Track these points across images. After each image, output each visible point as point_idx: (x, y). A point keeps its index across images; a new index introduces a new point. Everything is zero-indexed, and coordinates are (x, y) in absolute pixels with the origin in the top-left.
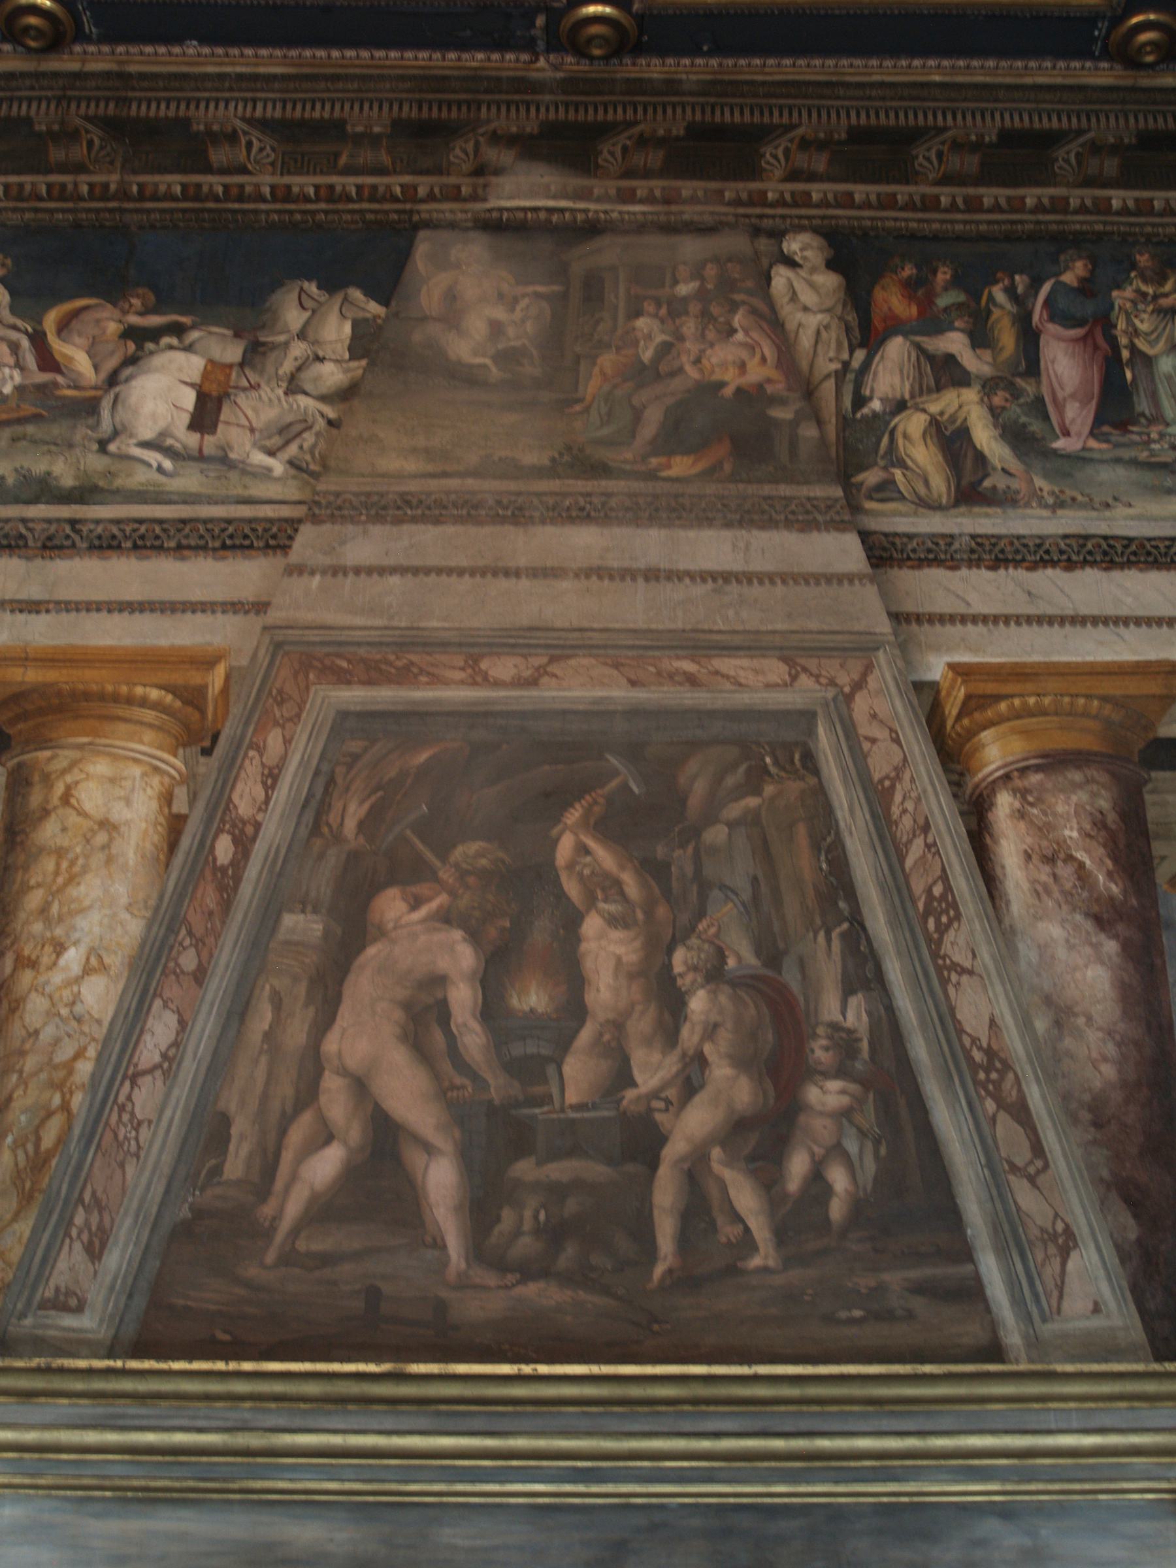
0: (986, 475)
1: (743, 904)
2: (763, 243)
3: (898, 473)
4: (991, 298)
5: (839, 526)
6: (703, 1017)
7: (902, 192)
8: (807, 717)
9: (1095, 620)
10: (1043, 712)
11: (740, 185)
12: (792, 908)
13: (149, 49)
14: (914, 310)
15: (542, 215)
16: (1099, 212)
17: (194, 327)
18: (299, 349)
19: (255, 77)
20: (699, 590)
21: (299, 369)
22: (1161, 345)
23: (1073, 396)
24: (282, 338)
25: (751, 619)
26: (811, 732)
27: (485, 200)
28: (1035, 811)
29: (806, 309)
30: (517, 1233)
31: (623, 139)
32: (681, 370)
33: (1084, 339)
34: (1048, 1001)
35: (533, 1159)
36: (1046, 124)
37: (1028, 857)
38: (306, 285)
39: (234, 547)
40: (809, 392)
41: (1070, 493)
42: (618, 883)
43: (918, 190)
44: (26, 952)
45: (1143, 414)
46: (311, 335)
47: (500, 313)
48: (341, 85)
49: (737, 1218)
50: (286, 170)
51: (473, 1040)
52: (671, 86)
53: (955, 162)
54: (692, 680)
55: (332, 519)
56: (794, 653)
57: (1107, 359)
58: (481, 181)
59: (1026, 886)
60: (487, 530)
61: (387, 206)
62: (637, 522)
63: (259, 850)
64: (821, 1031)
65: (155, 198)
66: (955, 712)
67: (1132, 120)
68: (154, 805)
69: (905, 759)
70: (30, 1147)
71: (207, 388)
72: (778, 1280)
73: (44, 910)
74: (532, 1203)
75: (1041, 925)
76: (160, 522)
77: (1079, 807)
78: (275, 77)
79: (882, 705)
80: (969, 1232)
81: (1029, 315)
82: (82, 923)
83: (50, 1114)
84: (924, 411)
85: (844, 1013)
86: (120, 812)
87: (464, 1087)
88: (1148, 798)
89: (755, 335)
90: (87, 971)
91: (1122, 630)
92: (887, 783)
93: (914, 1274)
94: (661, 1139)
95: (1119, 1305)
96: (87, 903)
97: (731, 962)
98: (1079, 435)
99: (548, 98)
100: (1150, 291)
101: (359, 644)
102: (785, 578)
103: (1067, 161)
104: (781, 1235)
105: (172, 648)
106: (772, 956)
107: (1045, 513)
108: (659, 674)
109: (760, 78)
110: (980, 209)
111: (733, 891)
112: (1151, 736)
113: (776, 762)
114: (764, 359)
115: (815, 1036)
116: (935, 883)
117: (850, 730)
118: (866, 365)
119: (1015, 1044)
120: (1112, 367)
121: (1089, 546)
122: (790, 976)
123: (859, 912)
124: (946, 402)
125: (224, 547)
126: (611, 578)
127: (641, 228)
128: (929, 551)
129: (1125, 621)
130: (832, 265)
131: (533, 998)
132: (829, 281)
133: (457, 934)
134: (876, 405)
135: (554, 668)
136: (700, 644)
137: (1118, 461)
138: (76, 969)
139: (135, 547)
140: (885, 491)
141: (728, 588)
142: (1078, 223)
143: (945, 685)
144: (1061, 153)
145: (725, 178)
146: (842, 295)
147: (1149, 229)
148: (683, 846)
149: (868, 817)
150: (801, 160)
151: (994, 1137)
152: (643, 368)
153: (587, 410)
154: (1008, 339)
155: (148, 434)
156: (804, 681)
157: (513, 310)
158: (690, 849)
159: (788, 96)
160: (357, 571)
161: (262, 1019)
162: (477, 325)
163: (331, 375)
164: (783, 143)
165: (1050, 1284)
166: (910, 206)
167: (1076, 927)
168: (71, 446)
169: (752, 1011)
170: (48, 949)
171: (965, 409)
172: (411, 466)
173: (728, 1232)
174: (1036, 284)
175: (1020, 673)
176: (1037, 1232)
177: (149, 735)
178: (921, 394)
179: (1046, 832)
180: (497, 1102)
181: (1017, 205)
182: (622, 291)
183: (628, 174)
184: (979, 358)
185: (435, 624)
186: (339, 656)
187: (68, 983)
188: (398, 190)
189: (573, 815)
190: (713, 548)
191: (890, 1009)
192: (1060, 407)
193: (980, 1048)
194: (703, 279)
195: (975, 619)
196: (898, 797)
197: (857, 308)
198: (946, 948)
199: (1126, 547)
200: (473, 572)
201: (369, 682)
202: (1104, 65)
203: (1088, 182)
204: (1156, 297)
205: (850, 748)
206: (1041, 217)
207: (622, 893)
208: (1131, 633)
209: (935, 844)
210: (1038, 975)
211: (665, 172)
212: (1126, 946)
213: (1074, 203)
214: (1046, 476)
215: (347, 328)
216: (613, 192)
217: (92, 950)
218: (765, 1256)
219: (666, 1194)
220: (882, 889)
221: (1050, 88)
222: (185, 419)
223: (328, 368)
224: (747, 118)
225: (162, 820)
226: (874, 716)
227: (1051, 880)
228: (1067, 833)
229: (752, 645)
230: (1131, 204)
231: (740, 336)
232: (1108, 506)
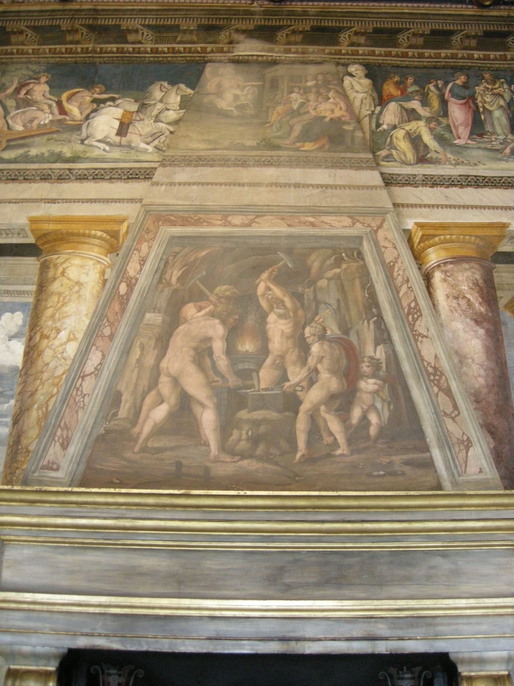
0: (428, 153)
1: (334, 309)
2: (340, 68)
3: (394, 152)
4: (429, 89)
5: (372, 168)
6: (317, 354)
7: (394, 51)
8: (360, 238)
9: (472, 207)
10: (452, 242)
11: (332, 48)
12: (354, 312)
15: (255, 58)
16: (469, 59)
17: (119, 99)
18: (160, 106)
19: (146, 10)
20: (316, 191)
21: (159, 113)
22: (495, 107)
23: (461, 124)
24: (153, 102)
25: (336, 202)
26: (361, 244)
28: (450, 279)
29: (357, 92)
30: (240, 440)
31: (286, 31)
32: (308, 112)
33: (465, 103)
35: (247, 410)
36: (448, 28)
37: (448, 297)
38: (163, 83)
39: (132, 178)
40: (359, 121)
41: (461, 159)
42: (282, 302)
44: (45, 333)
45: (488, 131)
46: (164, 100)
47: (238, 92)
48: (178, 13)
49: (331, 434)
50: (156, 42)
52: (305, 13)
53: (413, 41)
54: (313, 225)
55: (170, 165)
56: (354, 215)
57: (474, 112)
58: (232, 45)
59: (447, 308)
60: (231, 169)
61: (195, 55)
62: (291, 166)
63: (137, 289)
64: (366, 359)
65: (106, 52)
66: (418, 241)
67: (481, 26)
68: (98, 276)
69: (399, 255)
70: (44, 409)
71: (123, 120)
72: (348, 459)
73: (53, 316)
74: (246, 427)
75: (453, 323)
76: (104, 169)
79: (389, 234)
80: (428, 440)
82: (67, 321)
83: (52, 396)
84: (403, 129)
85: (375, 352)
86: (83, 279)
87: (218, 381)
88: (495, 275)
89: (338, 100)
90: (69, 340)
91: (483, 210)
92: (392, 264)
93: (405, 457)
94: (300, 403)
95: (490, 470)
96: (69, 314)
97: (329, 333)
98: (464, 138)
99: (257, 17)
100: (490, 87)
101: (180, 211)
102: (350, 187)
103: (456, 41)
104: (350, 441)
105: (107, 216)
108: (300, 222)
110: (424, 57)
111: (329, 305)
112: (495, 251)
113: (347, 255)
114: (341, 109)
115: (363, 362)
116: (412, 302)
117: (376, 244)
118: (381, 112)
119: (445, 365)
120: (476, 114)
121: (469, 179)
122: (353, 338)
123: (381, 313)
124: (412, 126)
125: (128, 178)
126: (281, 186)
128: (407, 180)
129: (484, 207)
130: (367, 76)
131: (247, 346)
132: (367, 82)
133: (217, 321)
134: (385, 127)
135: (256, 220)
136: (316, 211)
137: (480, 148)
138: (65, 340)
139: (94, 179)
140: (389, 158)
141: (327, 191)
142: (461, 63)
143: (413, 231)
144: (454, 38)
145: (326, 45)
146: (371, 86)
147: (488, 65)
148: (309, 287)
149: (384, 276)
150: (355, 39)
151: (437, 401)
152: (293, 111)
153: (271, 126)
154: (436, 103)
155: (100, 137)
156: (358, 225)
157: (243, 91)
158: (312, 289)
159: (349, 17)
160: (180, 184)
161: (136, 353)
162: (229, 96)
163: (172, 115)
164: (348, 33)
165: (462, 461)
166: (397, 56)
167: (467, 324)
168: (70, 142)
169: (337, 352)
170: (54, 331)
171: (420, 128)
172: (202, 146)
173: (328, 440)
174: (446, 83)
175: (443, 227)
176: (456, 440)
177: (96, 249)
178: (402, 123)
179: (454, 290)
180: (232, 387)
181: (438, 56)
182: (286, 84)
184: (425, 110)
185: (210, 203)
186: (171, 215)
187: (61, 345)
188: (199, 49)
189: (265, 275)
190: (321, 176)
191: (394, 351)
192: (456, 128)
193: (431, 367)
194: (317, 80)
195: (425, 206)
196: (396, 269)
197: (377, 92)
198: (417, 327)
199: (484, 180)
200: (225, 184)
201: (183, 225)
202: (470, 6)
203: (465, 48)
204: (492, 89)
205: (377, 250)
206: (447, 60)
207: (284, 305)
208: (486, 212)
209: (411, 287)
210: (452, 343)
211: (303, 43)
212: (487, 331)
213: (460, 56)
214: (452, 153)
215: (179, 98)
216: (282, 50)
217: (71, 332)
218: (343, 449)
219: (302, 425)
220: (391, 305)
221: (450, 15)
222: (115, 131)
223: (171, 112)
224: (334, 24)
225: (101, 281)
226: (386, 238)
227: (457, 306)
228: (463, 287)
229: (337, 212)
230: (481, 56)
231: (331, 100)
232: (476, 164)
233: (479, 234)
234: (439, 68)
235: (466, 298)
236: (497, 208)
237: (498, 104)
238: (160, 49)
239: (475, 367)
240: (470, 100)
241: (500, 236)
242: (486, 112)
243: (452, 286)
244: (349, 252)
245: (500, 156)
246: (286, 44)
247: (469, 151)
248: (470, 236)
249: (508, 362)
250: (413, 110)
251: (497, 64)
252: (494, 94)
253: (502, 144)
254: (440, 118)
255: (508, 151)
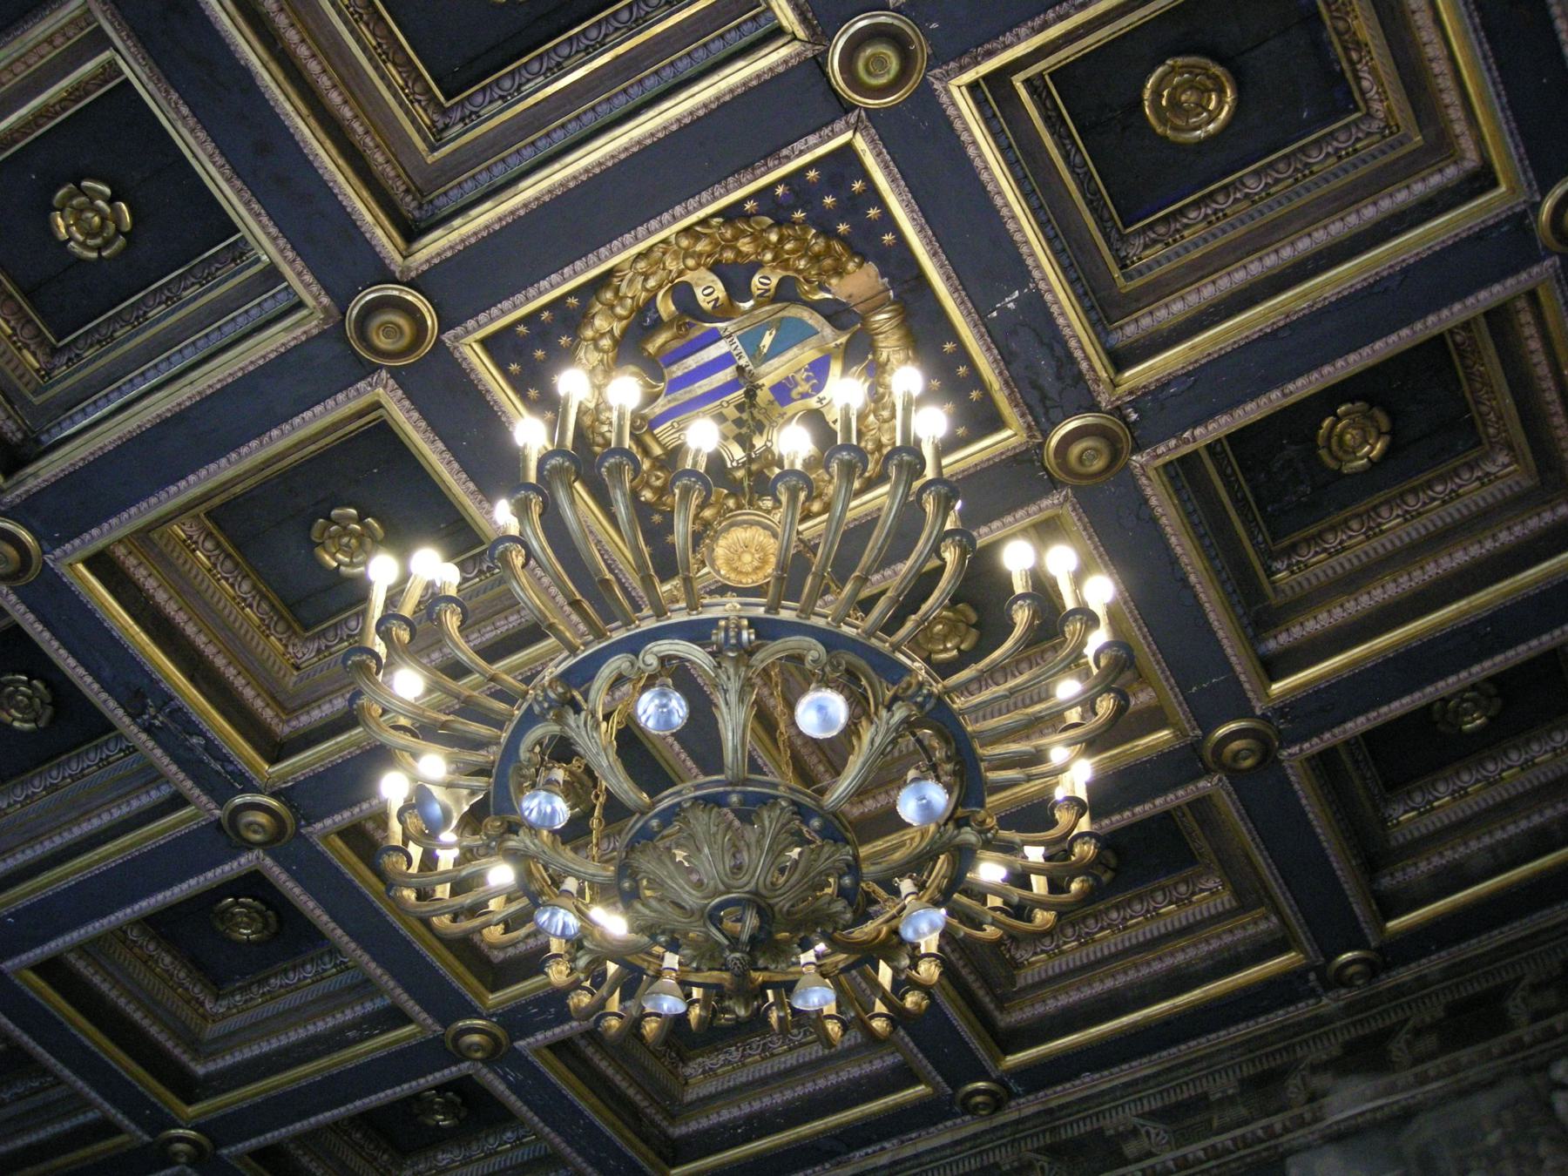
2: (1537, 1080)
11: (1500, 1039)
13: (1059, 1088)
19: (1135, 1082)
27: (1322, 1119)
31: (1403, 1036)
48: (1195, 1067)
52: (1422, 981)
58: (1315, 1105)
61: (1258, 1148)
78: (1146, 1079)
99: (1338, 1024)
109: (1480, 951)
183: (1418, 1061)
188: (1260, 1133)
216: (1411, 1079)
246: (1414, 1065)
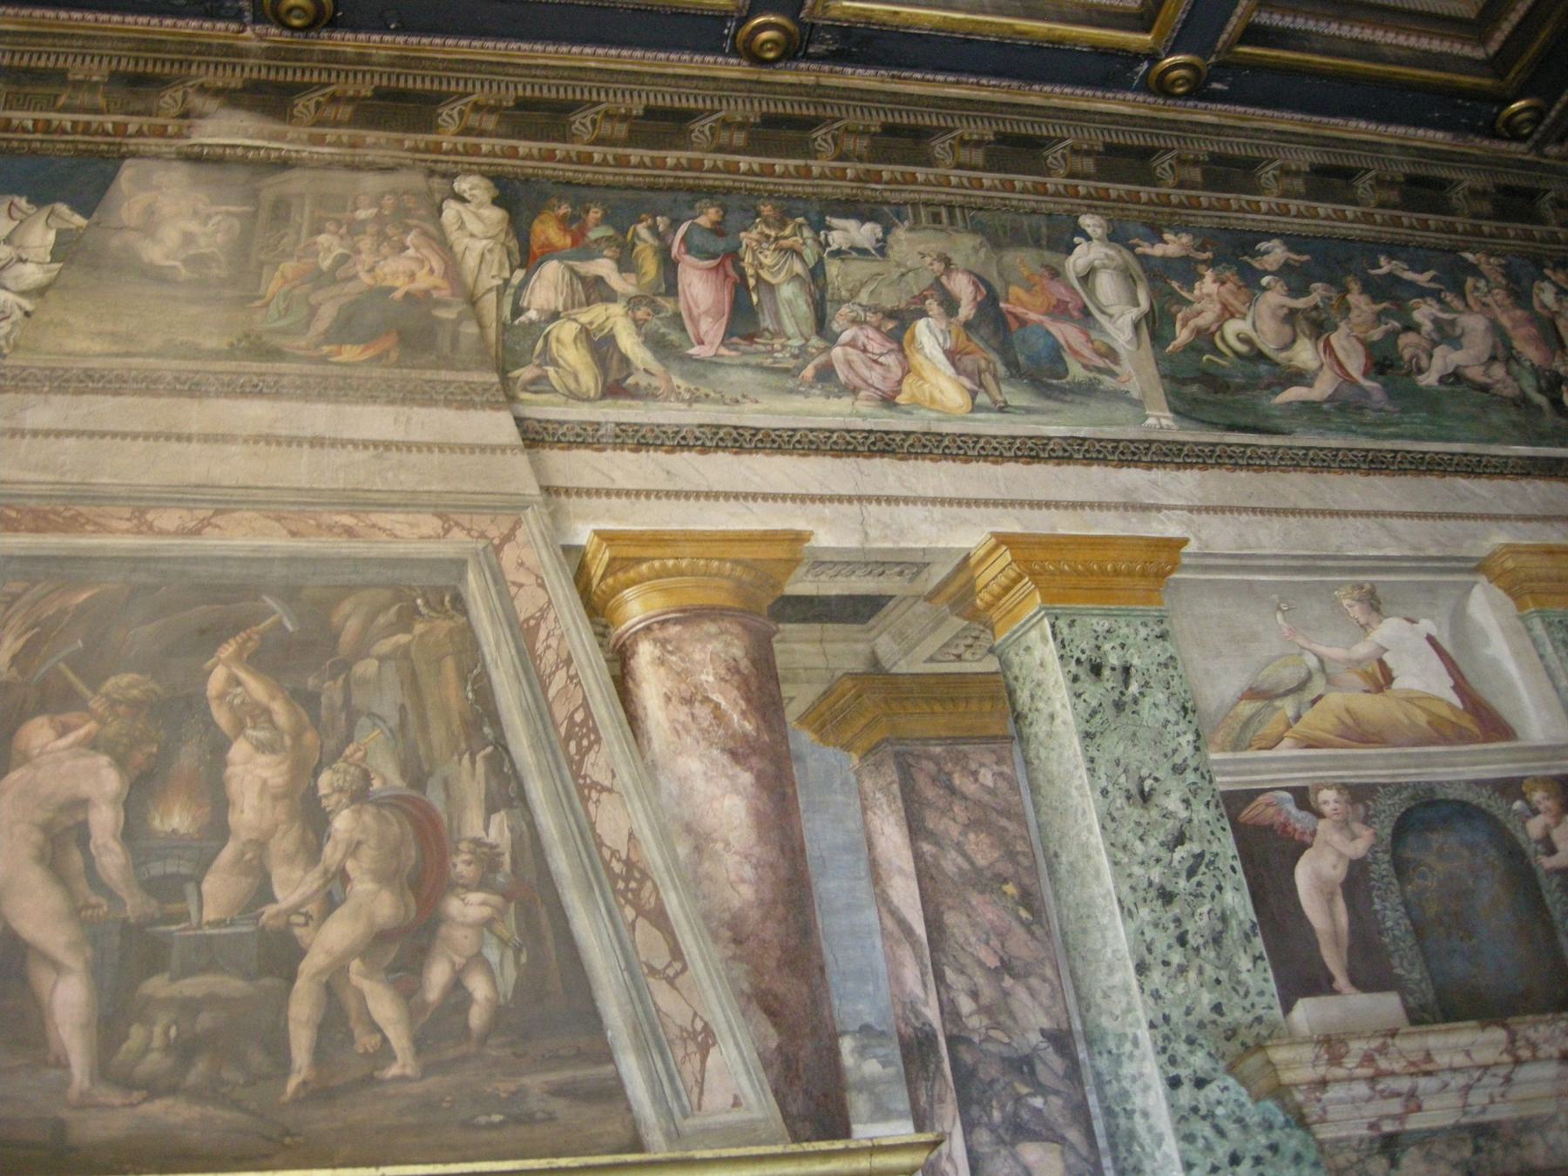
1: (391, 730)
2: (437, 182)
3: (551, 370)
4: (636, 235)
5: (495, 406)
6: (346, 835)
7: (560, 149)
8: (460, 565)
9: (727, 496)
10: (681, 574)
11: (419, 136)
12: (438, 734)
14: (569, 240)
15: (240, 151)
16: (729, 172)
20: (361, 456)
23: (706, 313)
25: (408, 481)
26: (462, 577)
27: (188, 137)
28: (674, 658)
29: (472, 235)
31: (316, 97)
32: (355, 277)
33: (716, 268)
34: (688, 829)
35: (167, 975)
36: (684, 104)
37: (668, 699)
38: (16, 199)
40: (473, 301)
41: (704, 390)
42: (267, 712)
43: (575, 148)
46: (17, 241)
47: (193, 226)
48: (66, 42)
49: (375, 1028)
51: (112, 859)
52: (362, 59)
53: (606, 128)
54: (350, 532)
55: (16, 389)
56: (448, 511)
57: (735, 284)
58: (187, 122)
59: (666, 725)
60: (163, 401)
61: (99, 139)
62: (306, 398)
64: (464, 846)
66: (600, 572)
69: (550, 602)
72: (416, 1088)
75: (680, 760)
77: (714, 656)
79: (529, 553)
80: (609, 1033)
81: (668, 249)
84: (575, 320)
85: (486, 828)
87: (98, 906)
88: (777, 647)
89: (426, 252)
91: (751, 503)
92: (532, 622)
93: (554, 1077)
94: (301, 953)
95: (759, 1101)
97: (376, 784)
98: (712, 344)
99: (252, 61)
100: (773, 234)
101: (30, 497)
102: (441, 447)
104: (419, 1044)
106: (417, 777)
107: (683, 406)
108: (319, 526)
109: (440, 56)
110: (628, 165)
111: (380, 718)
112: (778, 594)
113: (427, 603)
114: (432, 271)
115: (457, 851)
116: (577, 710)
117: (498, 577)
118: (524, 283)
119: (652, 854)
121: (721, 434)
122: (435, 797)
123: (503, 736)
124: (595, 314)
126: (279, 443)
127: (328, 165)
128: (578, 435)
130: (496, 202)
131: (176, 819)
132: (496, 215)
133: (104, 760)
134: (532, 314)
135: (217, 520)
136: (359, 501)
137: (746, 365)
140: (539, 384)
141: (388, 454)
142: (710, 179)
143: (591, 550)
144: (696, 126)
145: (406, 131)
146: (505, 225)
148: (334, 678)
149: (513, 651)
150: (473, 120)
151: (633, 942)
152: (321, 273)
153: (267, 305)
154: (650, 266)
156: (457, 534)
157: (206, 224)
158: (340, 681)
159: (464, 71)
160: (35, 433)
162: (171, 235)
163: (32, 274)
164: (458, 106)
165: (690, 1080)
166: (567, 159)
167: (713, 761)
169: (396, 829)
171: (612, 320)
173: (366, 1042)
174: (675, 223)
175: (659, 539)
176: (676, 1031)
178: (573, 307)
179: (684, 678)
182: (307, 210)
183: (320, 123)
185: (105, 480)
186: (8, 506)
188: (110, 127)
189: (228, 650)
190: (377, 421)
191: (532, 825)
192: (695, 322)
193: (619, 860)
194: (381, 207)
195: (618, 493)
196: (542, 634)
197: (518, 236)
198: (587, 768)
200: (147, 437)
201: (37, 530)
202: (733, 61)
203: (720, 149)
204: (777, 239)
205: (499, 593)
206: (680, 173)
207: (271, 721)
208: (759, 507)
209: (577, 675)
210: (679, 805)
211: (353, 122)
212: (759, 777)
213: (708, 164)
214: (683, 375)
215: (52, 236)
216: (305, 137)
218: (403, 1063)
219: (302, 1008)
220: (527, 720)
221: (687, 77)
224: (428, 86)
226: (521, 564)
228: (703, 677)
229: (410, 503)
230: (756, 167)
231: (411, 252)
233: (742, 556)
234: (660, 189)
235: (711, 700)
236: (784, 497)
237: (790, 270)
238: (15, 123)
239: (731, 860)
240: (727, 262)
241: (788, 561)
242: (762, 287)
243: (679, 674)
244: (432, 595)
245: (790, 383)
246: (314, 125)
247: (721, 373)
248: (720, 560)
249: (807, 845)
250: (599, 280)
251: (789, 186)
252: (780, 249)
253: (795, 357)
254: (659, 299)
255: (809, 372)
